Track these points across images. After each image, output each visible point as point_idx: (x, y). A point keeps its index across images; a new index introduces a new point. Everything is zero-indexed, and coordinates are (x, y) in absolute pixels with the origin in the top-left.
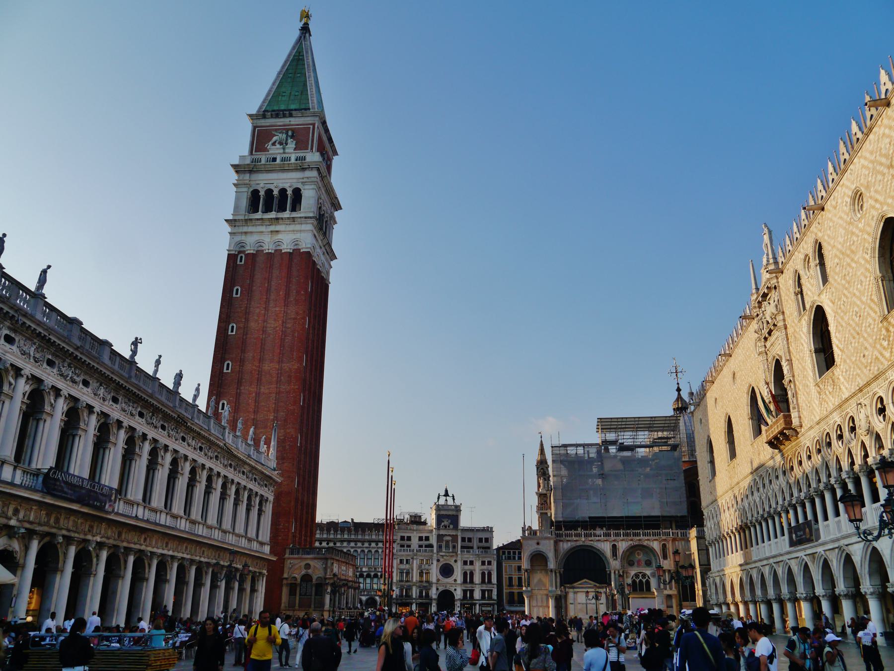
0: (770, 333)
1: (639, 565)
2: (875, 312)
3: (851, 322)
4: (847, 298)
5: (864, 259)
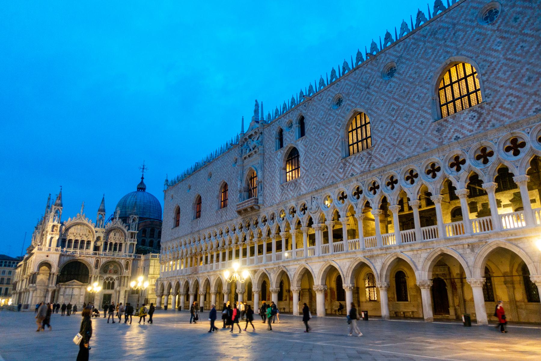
0: (249, 156)
1: (110, 272)
2: (338, 155)
3: (318, 157)
5: (336, 128)
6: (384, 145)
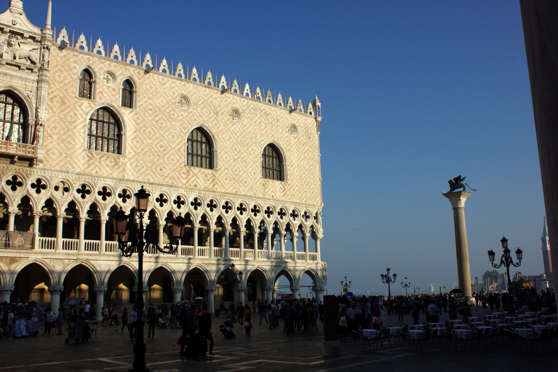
4: (154, 132)
6: (226, 174)
